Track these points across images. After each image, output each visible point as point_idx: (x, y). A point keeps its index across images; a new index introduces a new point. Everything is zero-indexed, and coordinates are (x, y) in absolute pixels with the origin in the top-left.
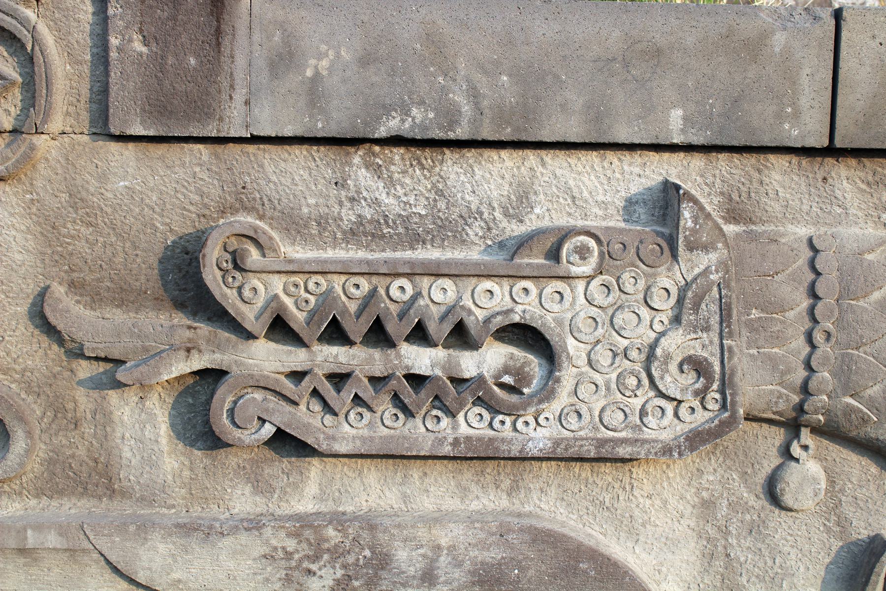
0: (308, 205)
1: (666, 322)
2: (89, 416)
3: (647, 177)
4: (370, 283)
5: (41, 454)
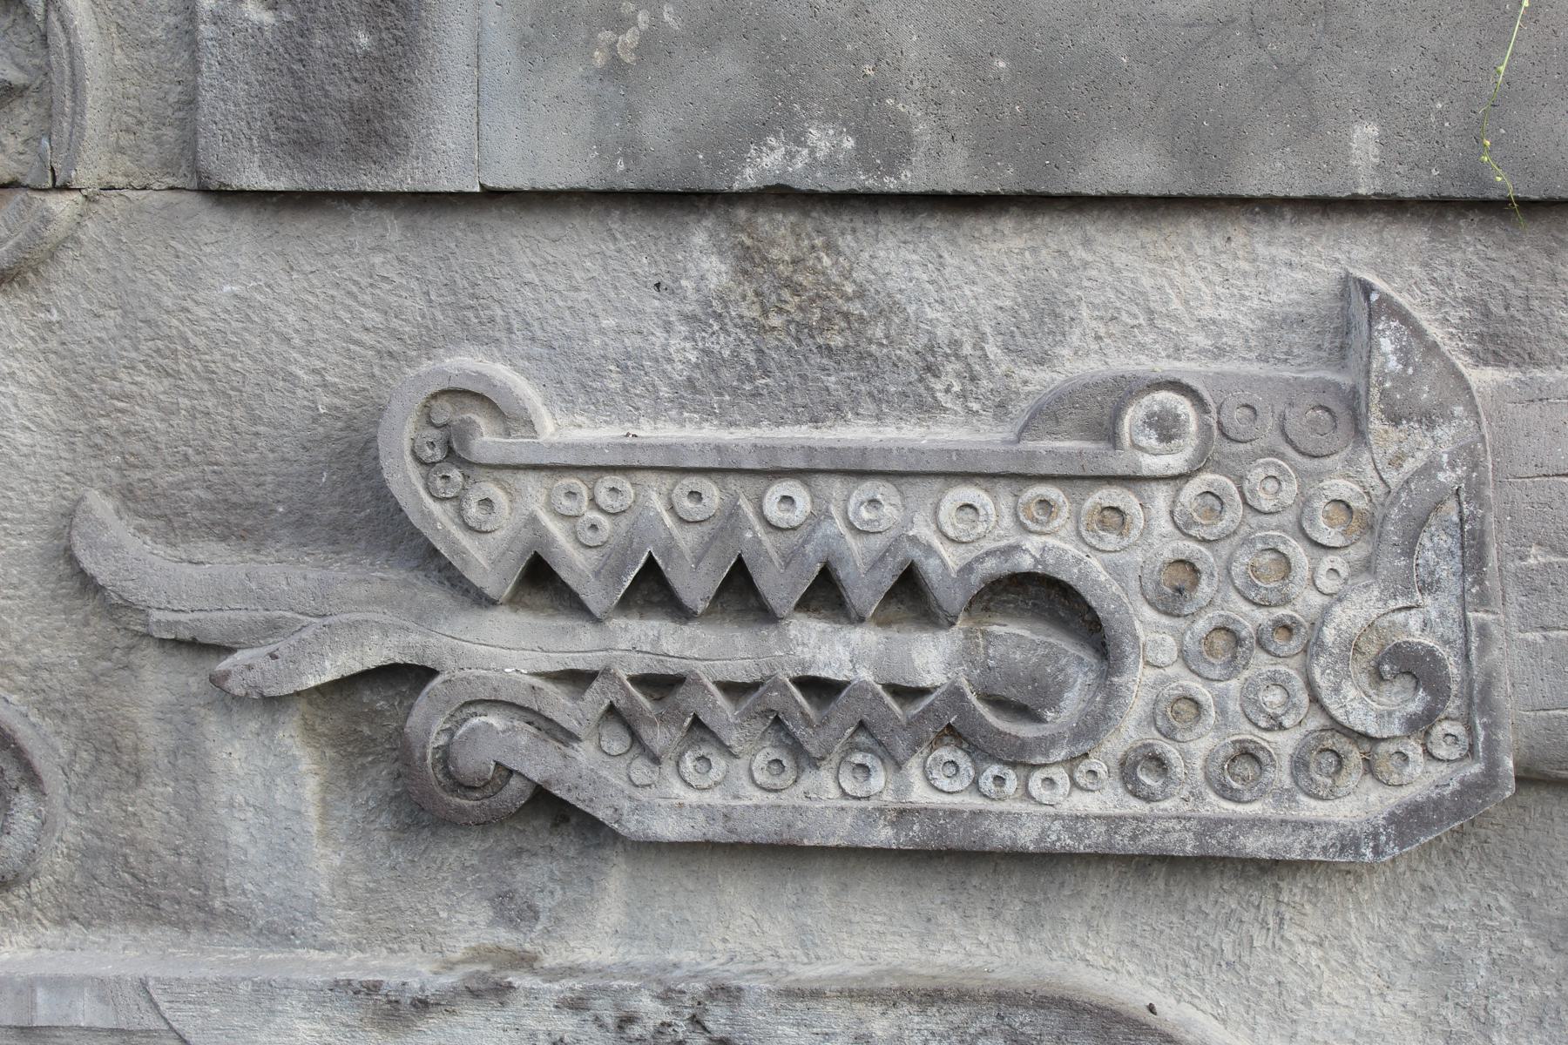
0: (602, 332)
1: (1344, 572)
3: (1305, 267)
4: (723, 489)
5: (68, 837)
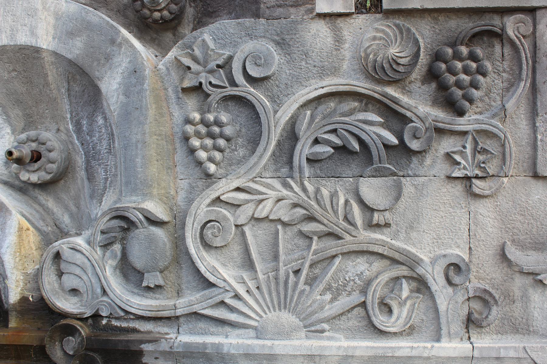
2: (519, 298)
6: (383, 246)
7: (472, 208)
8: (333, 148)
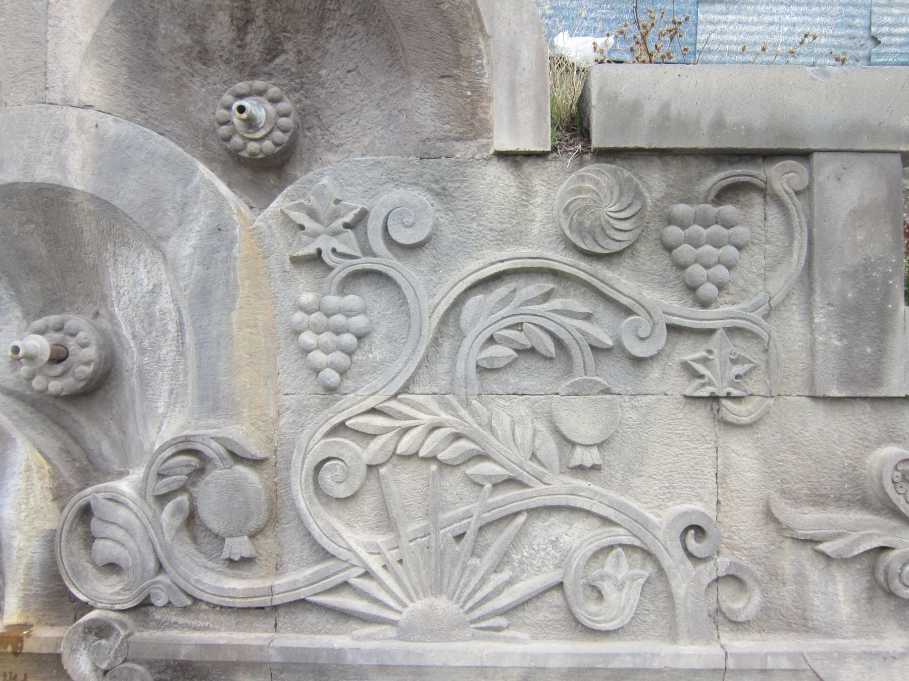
6: (589, 498)
7: (720, 442)
8: (517, 351)
